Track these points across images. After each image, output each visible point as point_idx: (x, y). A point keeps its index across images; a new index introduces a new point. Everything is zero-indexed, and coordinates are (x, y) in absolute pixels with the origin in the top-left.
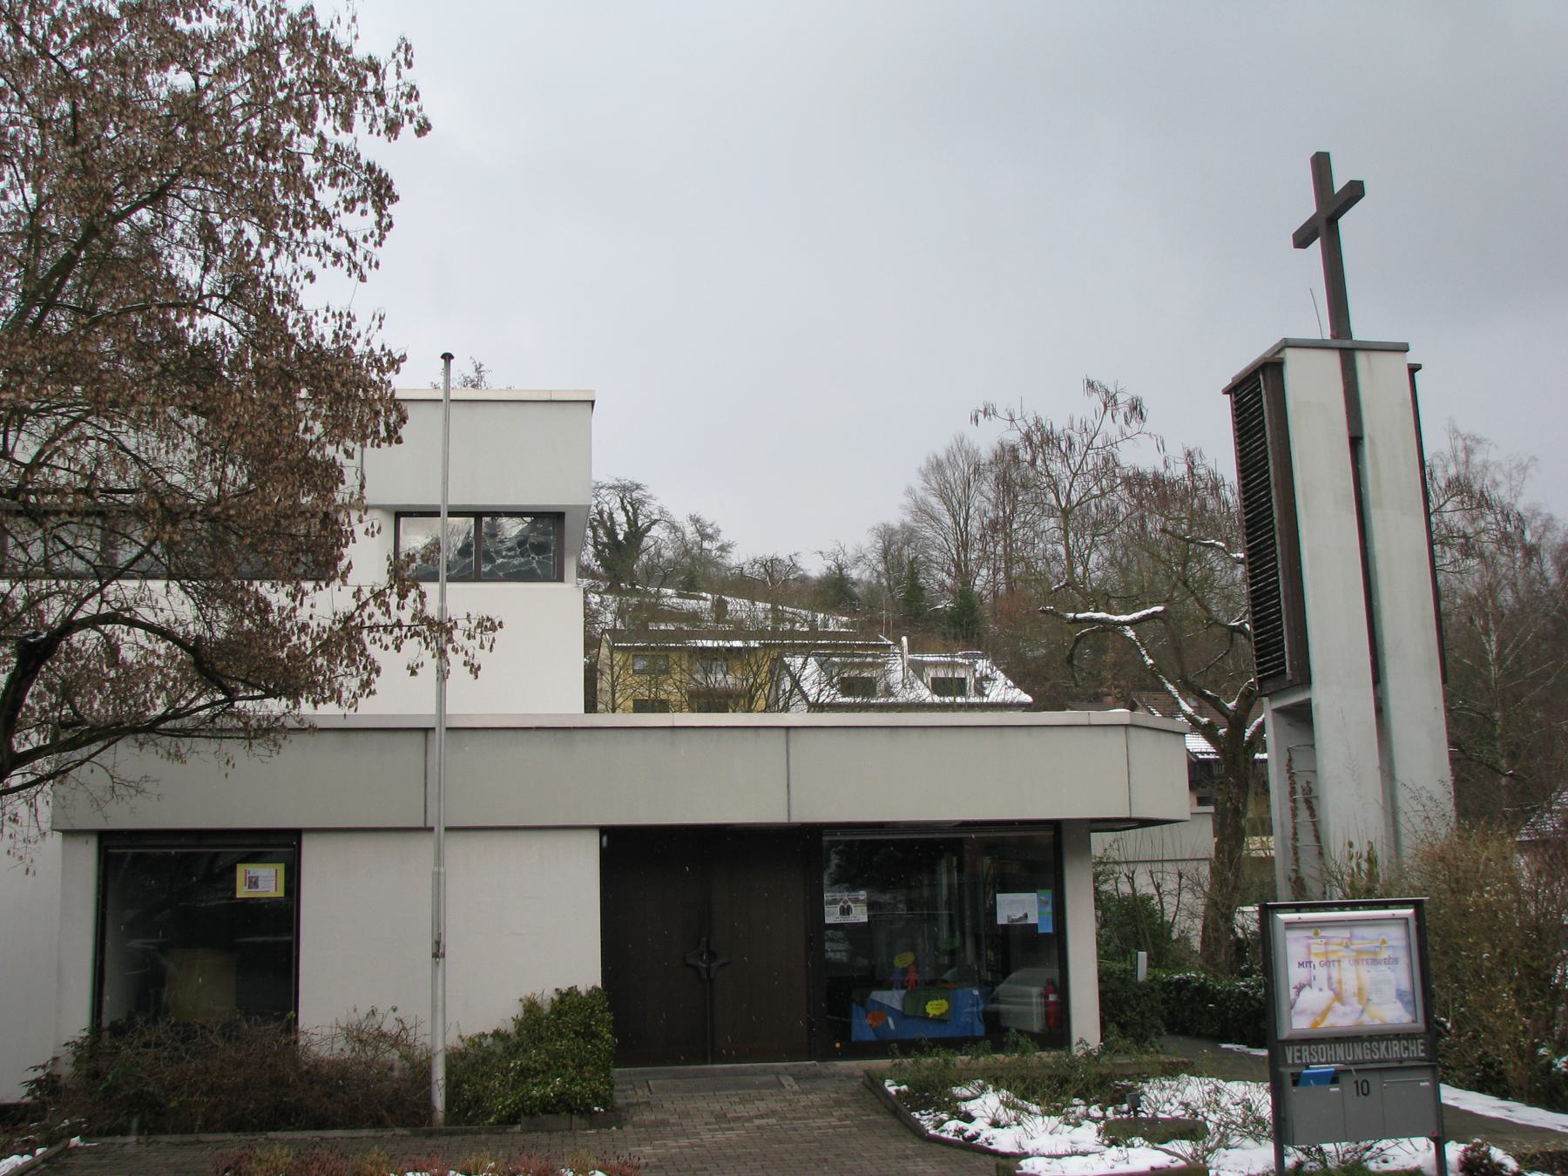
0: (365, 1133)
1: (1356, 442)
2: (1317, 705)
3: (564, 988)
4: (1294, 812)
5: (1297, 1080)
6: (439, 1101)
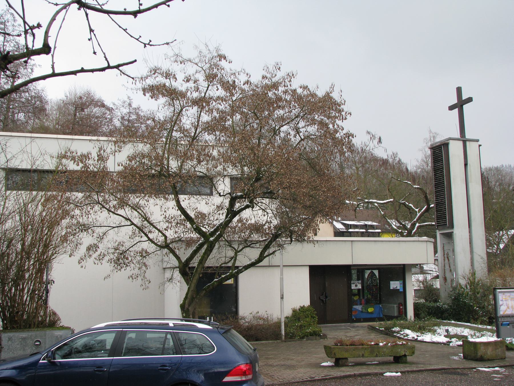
0: (270, 341)
1: (466, 165)
2: (455, 234)
3: (302, 306)
4: (444, 259)
5: (502, 324)
6: (283, 332)
